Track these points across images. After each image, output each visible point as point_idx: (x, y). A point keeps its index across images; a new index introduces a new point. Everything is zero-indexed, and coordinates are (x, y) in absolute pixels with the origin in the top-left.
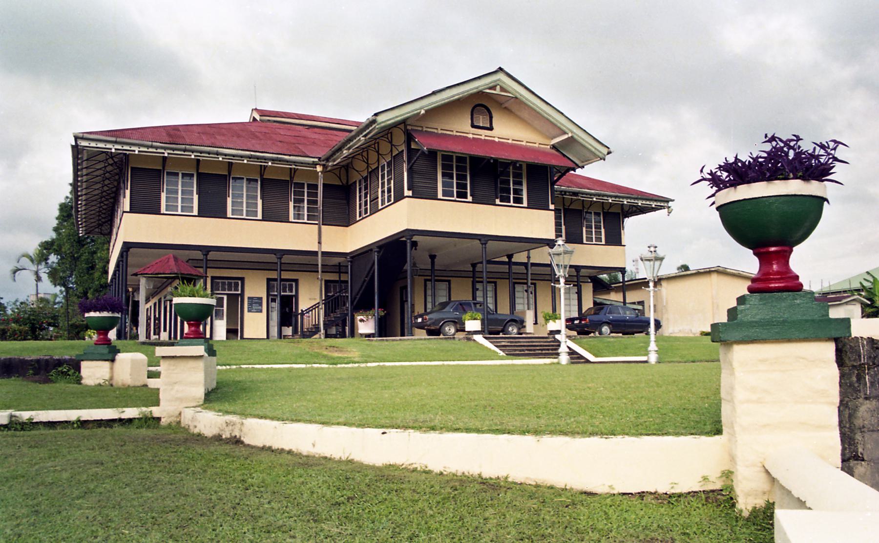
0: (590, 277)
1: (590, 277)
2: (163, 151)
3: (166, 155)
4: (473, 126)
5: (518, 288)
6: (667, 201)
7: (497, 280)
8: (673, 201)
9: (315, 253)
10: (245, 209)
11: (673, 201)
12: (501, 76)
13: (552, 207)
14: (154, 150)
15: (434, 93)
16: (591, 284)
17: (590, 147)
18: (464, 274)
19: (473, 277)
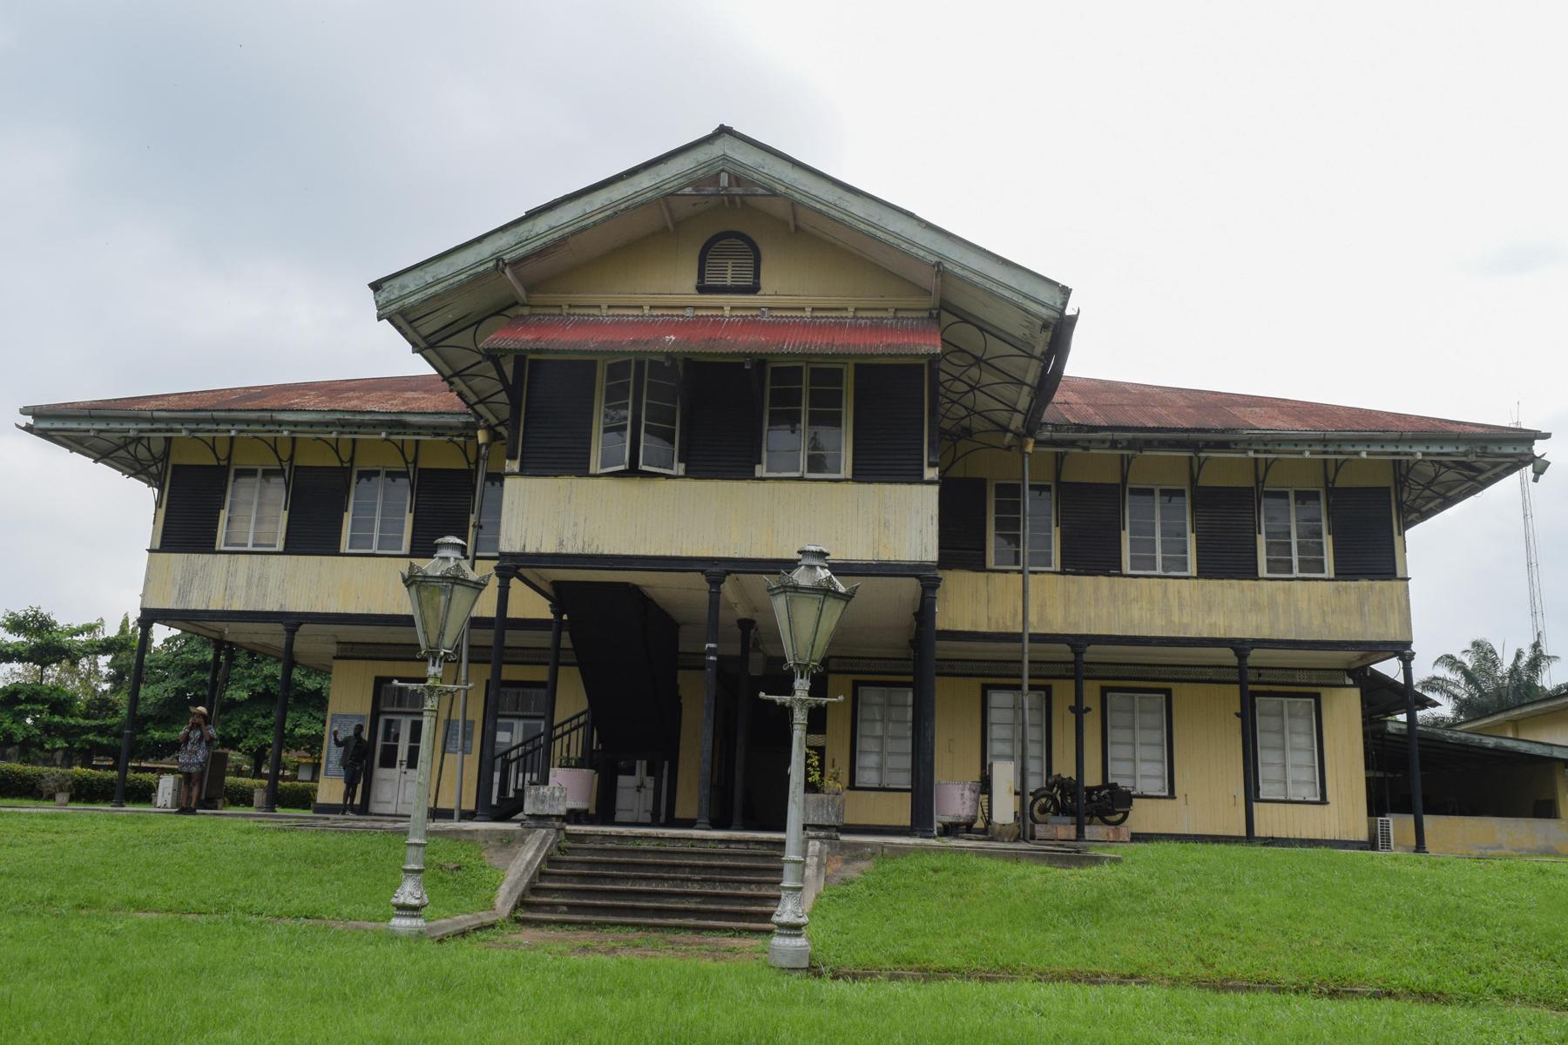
0: (1350, 672)
1: (1350, 672)
2: (179, 426)
3: (233, 433)
4: (702, 289)
5: (998, 699)
6: (1529, 437)
7: (1319, 690)
8: (1547, 436)
9: (1016, 638)
10: (376, 534)
11: (1547, 436)
12: (722, 147)
13: (931, 473)
14: (148, 426)
15: (532, 215)
16: (1356, 692)
17: (1007, 294)
18: (1211, 673)
19: (1242, 682)
